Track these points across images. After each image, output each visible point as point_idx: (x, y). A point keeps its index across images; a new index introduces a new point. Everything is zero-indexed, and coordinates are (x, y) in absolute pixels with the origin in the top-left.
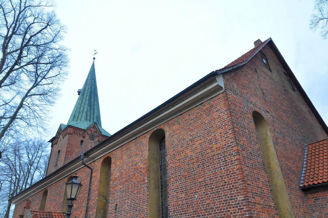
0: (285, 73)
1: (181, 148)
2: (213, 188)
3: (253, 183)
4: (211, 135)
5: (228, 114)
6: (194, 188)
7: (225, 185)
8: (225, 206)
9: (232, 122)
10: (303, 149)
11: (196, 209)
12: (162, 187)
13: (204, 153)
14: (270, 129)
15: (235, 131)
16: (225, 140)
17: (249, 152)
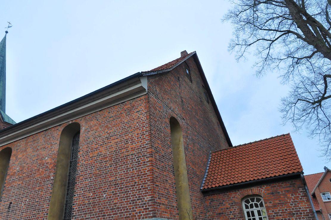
0: (203, 86)
1: (95, 145)
2: (123, 188)
3: (161, 185)
4: (128, 135)
5: (147, 116)
6: (104, 187)
7: (134, 185)
8: (132, 206)
9: (150, 125)
11: (102, 208)
12: (69, 184)
13: (119, 152)
14: (183, 135)
15: (152, 133)
16: (141, 142)
17: (162, 155)
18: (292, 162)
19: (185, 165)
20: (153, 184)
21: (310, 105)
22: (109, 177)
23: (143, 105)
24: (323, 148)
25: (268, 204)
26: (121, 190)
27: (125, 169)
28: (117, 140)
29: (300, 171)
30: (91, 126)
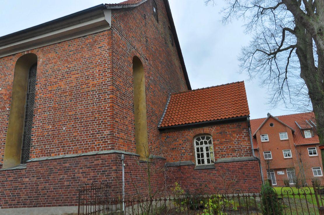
0: (169, 26)
1: (54, 78)
2: (83, 122)
4: (89, 71)
5: (109, 53)
6: (63, 121)
7: (95, 120)
8: (92, 139)
9: (112, 62)
10: (168, 97)
11: (62, 140)
12: (27, 116)
13: (79, 87)
15: (114, 71)
16: (102, 78)
18: (242, 107)
19: (144, 104)
20: (113, 120)
21: (266, 56)
22: (69, 111)
23: (107, 41)
24: (270, 97)
25: (216, 142)
26: (81, 124)
27: (86, 105)
28: (77, 76)
29: (247, 114)
30: (49, 58)
